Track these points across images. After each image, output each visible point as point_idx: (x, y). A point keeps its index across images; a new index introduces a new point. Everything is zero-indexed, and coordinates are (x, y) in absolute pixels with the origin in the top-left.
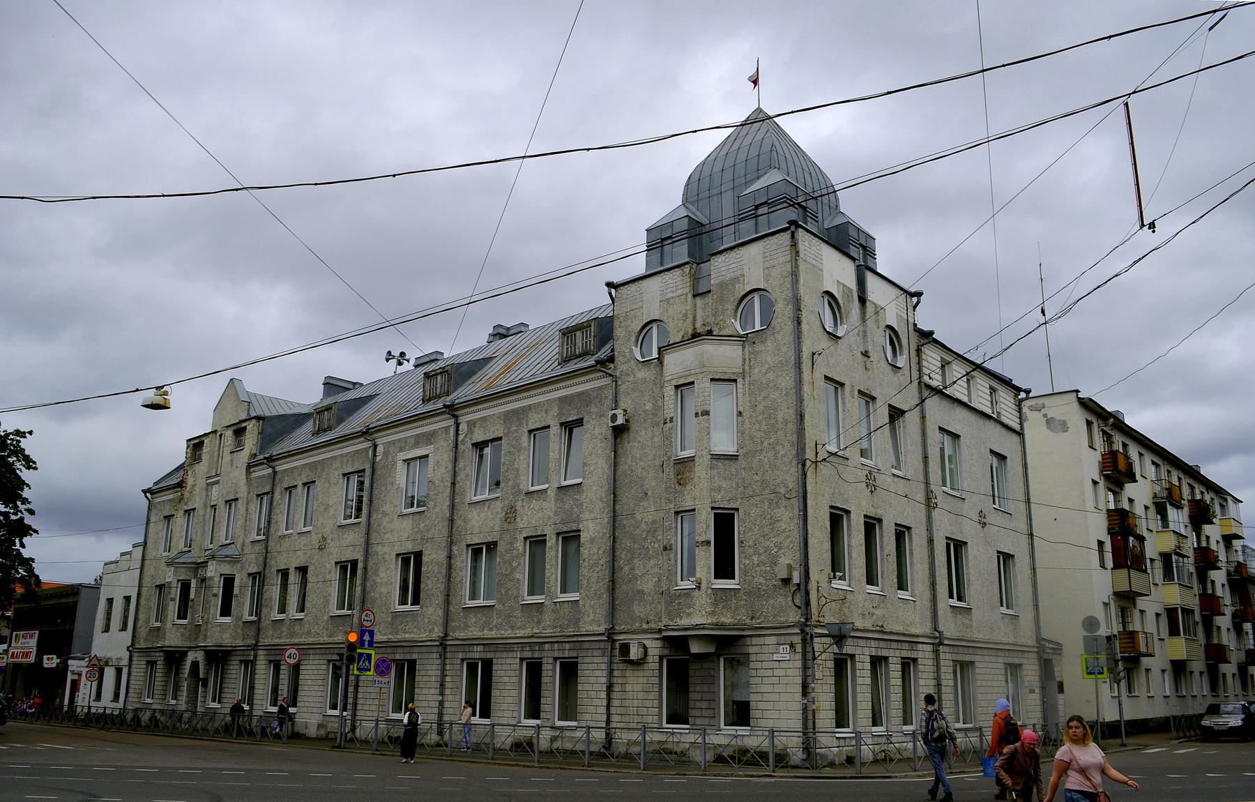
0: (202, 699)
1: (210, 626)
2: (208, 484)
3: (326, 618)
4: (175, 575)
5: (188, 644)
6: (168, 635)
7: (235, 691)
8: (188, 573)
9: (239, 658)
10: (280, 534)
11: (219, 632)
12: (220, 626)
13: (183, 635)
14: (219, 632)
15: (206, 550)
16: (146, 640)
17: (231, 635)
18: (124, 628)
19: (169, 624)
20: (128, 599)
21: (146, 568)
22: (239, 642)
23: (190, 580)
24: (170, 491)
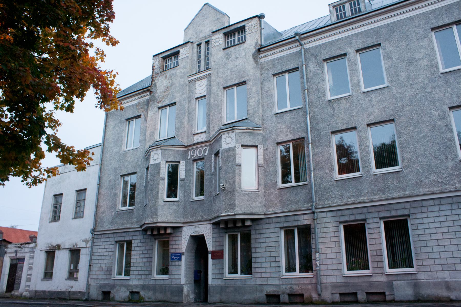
0: (217, 271)
1: (237, 195)
2: (190, 82)
3: (450, 164)
4: (163, 157)
5: (182, 220)
6: (160, 212)
7: (277, 259)
8: (176, 155)
9: (278, 225)
10: (326, 99)
11: (248, 200)
12: (247, 194)
13: (176, 212)
14: (248, 200)
15: (194, 135)
16: (112, 223)
17: (260, 203)
18: (78, 214)
19: (160, 202)
20: (81, 192)
21: (105, 163)
22: (276, 209)
23: (179, 162)
24: (137, 97)
